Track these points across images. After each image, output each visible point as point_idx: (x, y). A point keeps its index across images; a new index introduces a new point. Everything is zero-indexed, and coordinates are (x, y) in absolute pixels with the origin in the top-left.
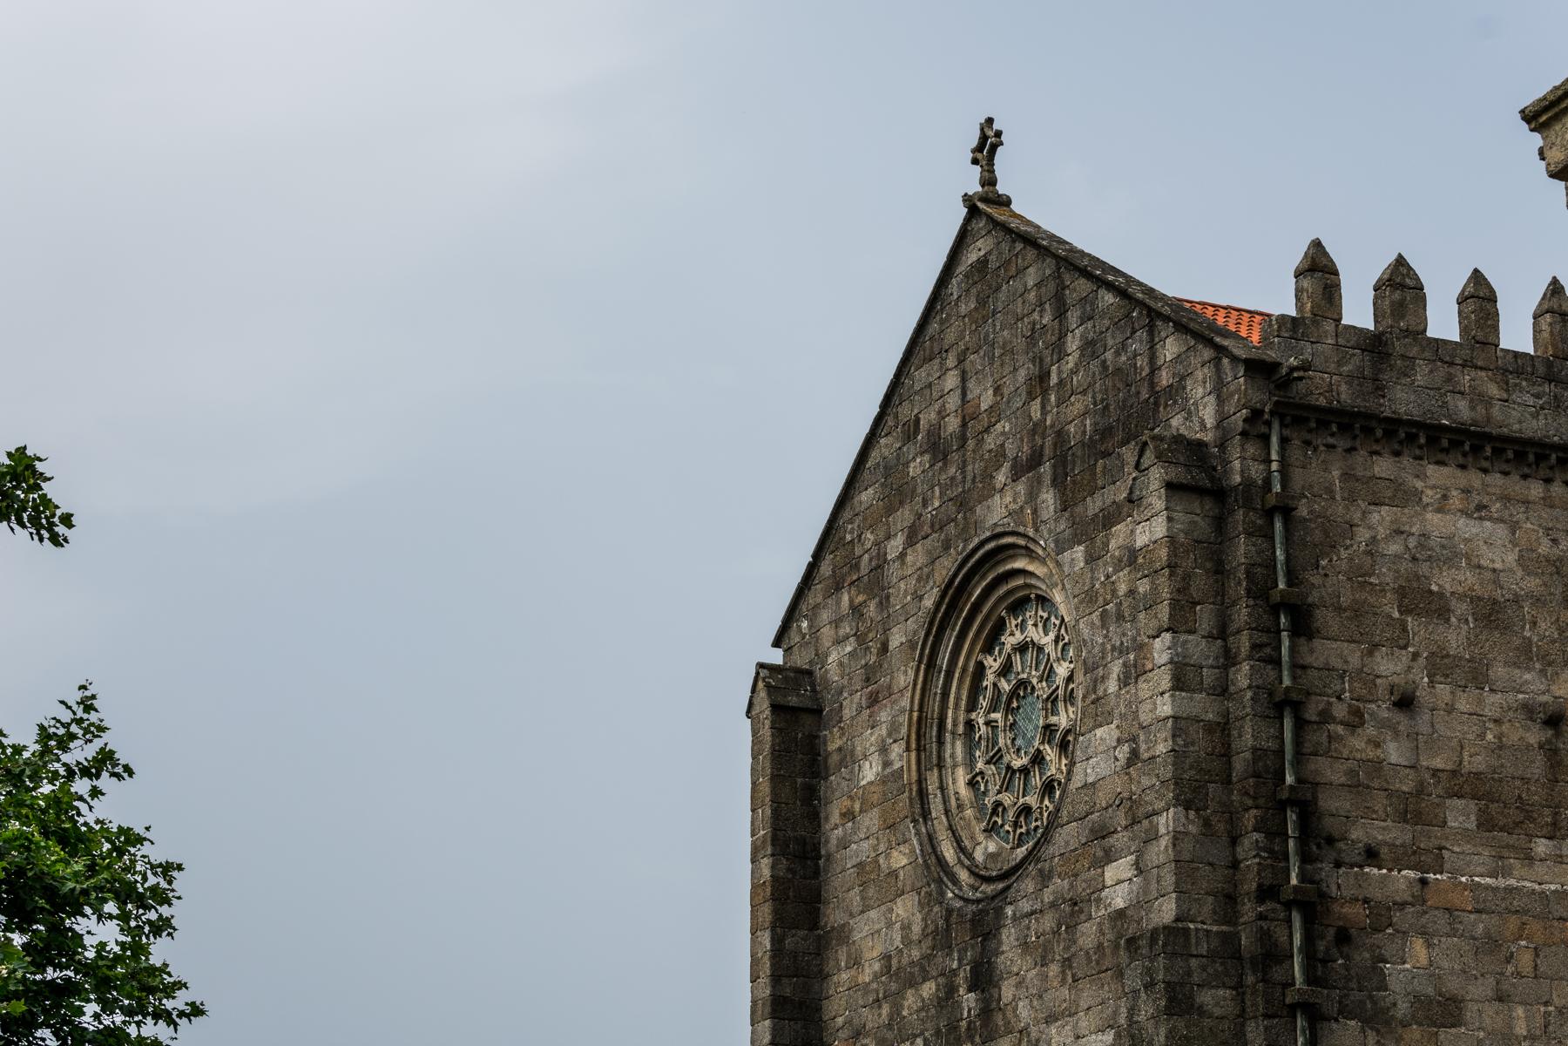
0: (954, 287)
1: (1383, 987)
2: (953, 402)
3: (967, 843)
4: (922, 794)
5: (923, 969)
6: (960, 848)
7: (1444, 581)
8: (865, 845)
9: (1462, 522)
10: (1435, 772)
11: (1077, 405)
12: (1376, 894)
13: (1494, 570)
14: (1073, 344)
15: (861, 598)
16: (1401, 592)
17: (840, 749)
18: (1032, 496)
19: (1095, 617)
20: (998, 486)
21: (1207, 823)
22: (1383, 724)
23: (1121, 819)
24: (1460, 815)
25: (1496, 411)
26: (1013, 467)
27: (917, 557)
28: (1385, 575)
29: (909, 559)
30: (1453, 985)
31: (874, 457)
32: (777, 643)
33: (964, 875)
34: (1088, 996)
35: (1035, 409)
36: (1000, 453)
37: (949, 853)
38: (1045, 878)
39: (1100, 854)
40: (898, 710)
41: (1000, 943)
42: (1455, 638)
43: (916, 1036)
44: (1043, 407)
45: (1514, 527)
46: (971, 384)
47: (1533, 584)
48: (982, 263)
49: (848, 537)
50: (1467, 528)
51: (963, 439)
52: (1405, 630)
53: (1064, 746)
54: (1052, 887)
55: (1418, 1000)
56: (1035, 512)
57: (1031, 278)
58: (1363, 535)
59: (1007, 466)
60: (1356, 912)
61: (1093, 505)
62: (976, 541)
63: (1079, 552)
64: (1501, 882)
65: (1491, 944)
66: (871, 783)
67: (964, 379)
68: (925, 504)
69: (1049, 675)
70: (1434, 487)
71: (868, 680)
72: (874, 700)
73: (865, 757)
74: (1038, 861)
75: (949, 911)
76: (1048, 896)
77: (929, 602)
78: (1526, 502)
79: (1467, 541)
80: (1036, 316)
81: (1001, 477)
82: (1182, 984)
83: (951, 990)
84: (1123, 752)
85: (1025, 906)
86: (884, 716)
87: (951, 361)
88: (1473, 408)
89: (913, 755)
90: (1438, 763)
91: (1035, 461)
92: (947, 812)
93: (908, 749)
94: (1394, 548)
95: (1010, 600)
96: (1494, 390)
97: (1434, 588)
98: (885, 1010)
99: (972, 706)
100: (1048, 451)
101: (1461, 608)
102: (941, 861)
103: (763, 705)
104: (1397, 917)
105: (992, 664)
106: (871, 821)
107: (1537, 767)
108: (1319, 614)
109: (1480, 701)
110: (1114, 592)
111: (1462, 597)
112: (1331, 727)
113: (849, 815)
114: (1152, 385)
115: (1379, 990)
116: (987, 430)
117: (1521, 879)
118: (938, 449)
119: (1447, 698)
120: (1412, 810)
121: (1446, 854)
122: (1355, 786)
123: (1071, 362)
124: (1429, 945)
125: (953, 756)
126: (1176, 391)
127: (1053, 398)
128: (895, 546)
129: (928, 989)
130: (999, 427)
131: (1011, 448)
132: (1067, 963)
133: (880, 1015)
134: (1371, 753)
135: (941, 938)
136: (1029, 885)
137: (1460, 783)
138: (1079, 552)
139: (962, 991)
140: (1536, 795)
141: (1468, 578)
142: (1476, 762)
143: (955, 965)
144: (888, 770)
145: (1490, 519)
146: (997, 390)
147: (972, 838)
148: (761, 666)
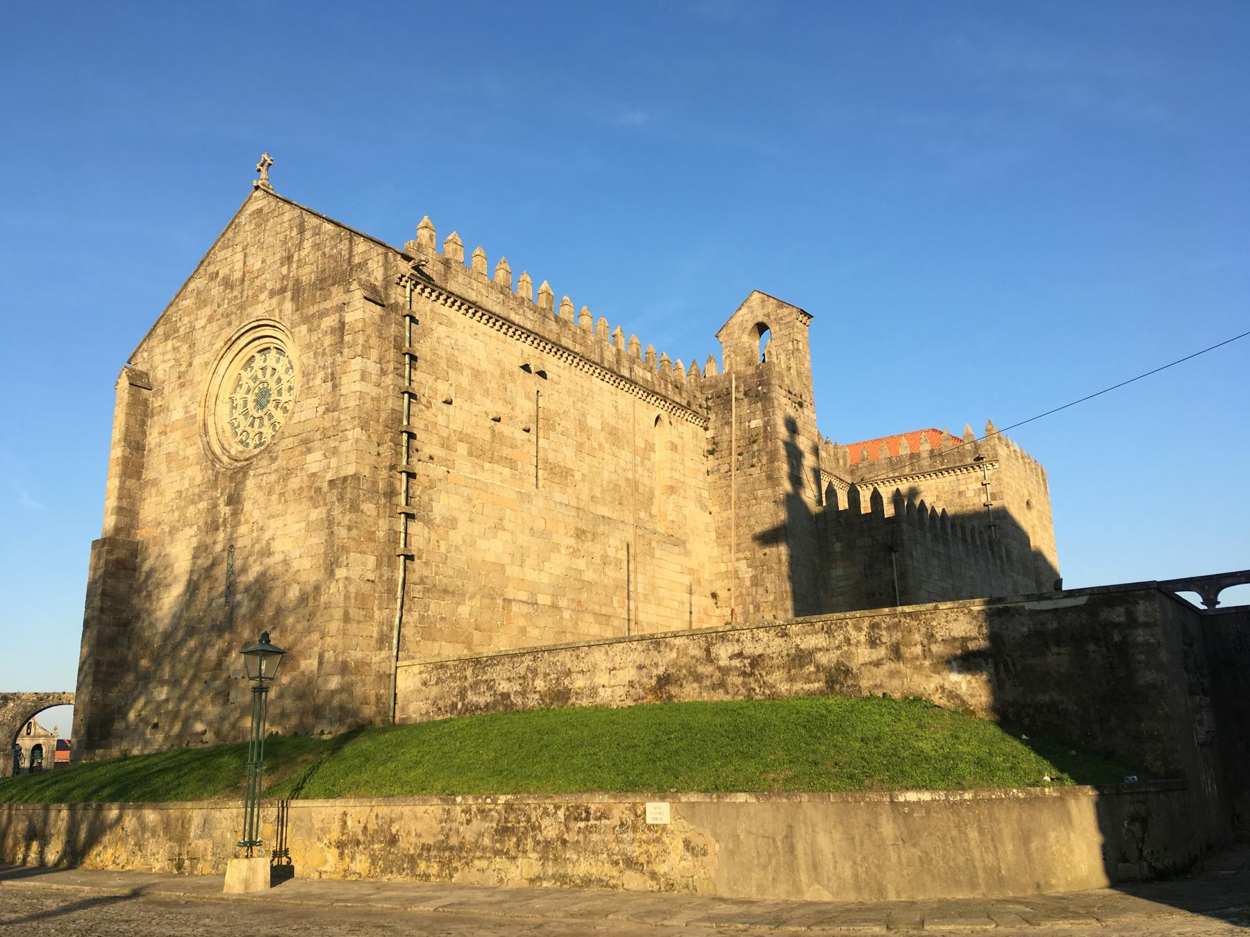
2: (239, 265)
3: (227, 446)
5: (200, 496)
7: (462, 359)
11: (308, 269)
14: (307, 245)
15: (179, 344)
17: (161, 406)
18: (280, 304)
19: (311, 355)
21: (369, 436)
22: (439, 409)
23: (318, 435)
24: (462, 448)
27: (214, 327)
29: (207, 329)
30: (456, 513)
33: (225, 459)
34: (293, 507)
35: (284, 270)
36: (262, 288)
37: (218, 450)
39: (305, 450)
41: (245, 486)
43: (192, 525)
44: (289, 269)
45: (486, 345)
46: (248, 259)
48: (260, 211)
49: (174, 319)
50: (471, 341)
51: (243, 280)
53: (285, 410)
54: (276, 463)
56: (280, 311)
57: (286, 217)
58: (436, 334)
59: (266, 293)
61: (313, 310)
62: (247, 322)
63: (304, 328)
64: (474, 476)
67: (245, 256)
68: (219, 306)
71: (179, 377)
72: (182, 385)
73: (175, 409)
74: (270, 452)
75: (218, 473)
78: (491, 337)
80: (288, 233)
83: (215, 506)
87: (239, 248)
88: (477, 296)
91: (283, 290)
94: (447, 342)
96: (484, 292)
98: (177, 514)
100: (290, 287)
102: (213, 453)
104: (438, 484)
107: (488, 437)
110: (322, 345)
114: (349, 262)
116: (257, 278)
120: (446, 444)
126: (362, 265)
127: (295, 266)
130: (263, 276)
131: (269, 285)
133: (173, 516)
134: (434, 419)
135: (214, 484)
136: (265, 462)
137: (463, 437)
139: (221, 506)
142: (469, 430)
143: (219, 495)
144: (188, 415)
146: (263, 261)
147: (230, 445)
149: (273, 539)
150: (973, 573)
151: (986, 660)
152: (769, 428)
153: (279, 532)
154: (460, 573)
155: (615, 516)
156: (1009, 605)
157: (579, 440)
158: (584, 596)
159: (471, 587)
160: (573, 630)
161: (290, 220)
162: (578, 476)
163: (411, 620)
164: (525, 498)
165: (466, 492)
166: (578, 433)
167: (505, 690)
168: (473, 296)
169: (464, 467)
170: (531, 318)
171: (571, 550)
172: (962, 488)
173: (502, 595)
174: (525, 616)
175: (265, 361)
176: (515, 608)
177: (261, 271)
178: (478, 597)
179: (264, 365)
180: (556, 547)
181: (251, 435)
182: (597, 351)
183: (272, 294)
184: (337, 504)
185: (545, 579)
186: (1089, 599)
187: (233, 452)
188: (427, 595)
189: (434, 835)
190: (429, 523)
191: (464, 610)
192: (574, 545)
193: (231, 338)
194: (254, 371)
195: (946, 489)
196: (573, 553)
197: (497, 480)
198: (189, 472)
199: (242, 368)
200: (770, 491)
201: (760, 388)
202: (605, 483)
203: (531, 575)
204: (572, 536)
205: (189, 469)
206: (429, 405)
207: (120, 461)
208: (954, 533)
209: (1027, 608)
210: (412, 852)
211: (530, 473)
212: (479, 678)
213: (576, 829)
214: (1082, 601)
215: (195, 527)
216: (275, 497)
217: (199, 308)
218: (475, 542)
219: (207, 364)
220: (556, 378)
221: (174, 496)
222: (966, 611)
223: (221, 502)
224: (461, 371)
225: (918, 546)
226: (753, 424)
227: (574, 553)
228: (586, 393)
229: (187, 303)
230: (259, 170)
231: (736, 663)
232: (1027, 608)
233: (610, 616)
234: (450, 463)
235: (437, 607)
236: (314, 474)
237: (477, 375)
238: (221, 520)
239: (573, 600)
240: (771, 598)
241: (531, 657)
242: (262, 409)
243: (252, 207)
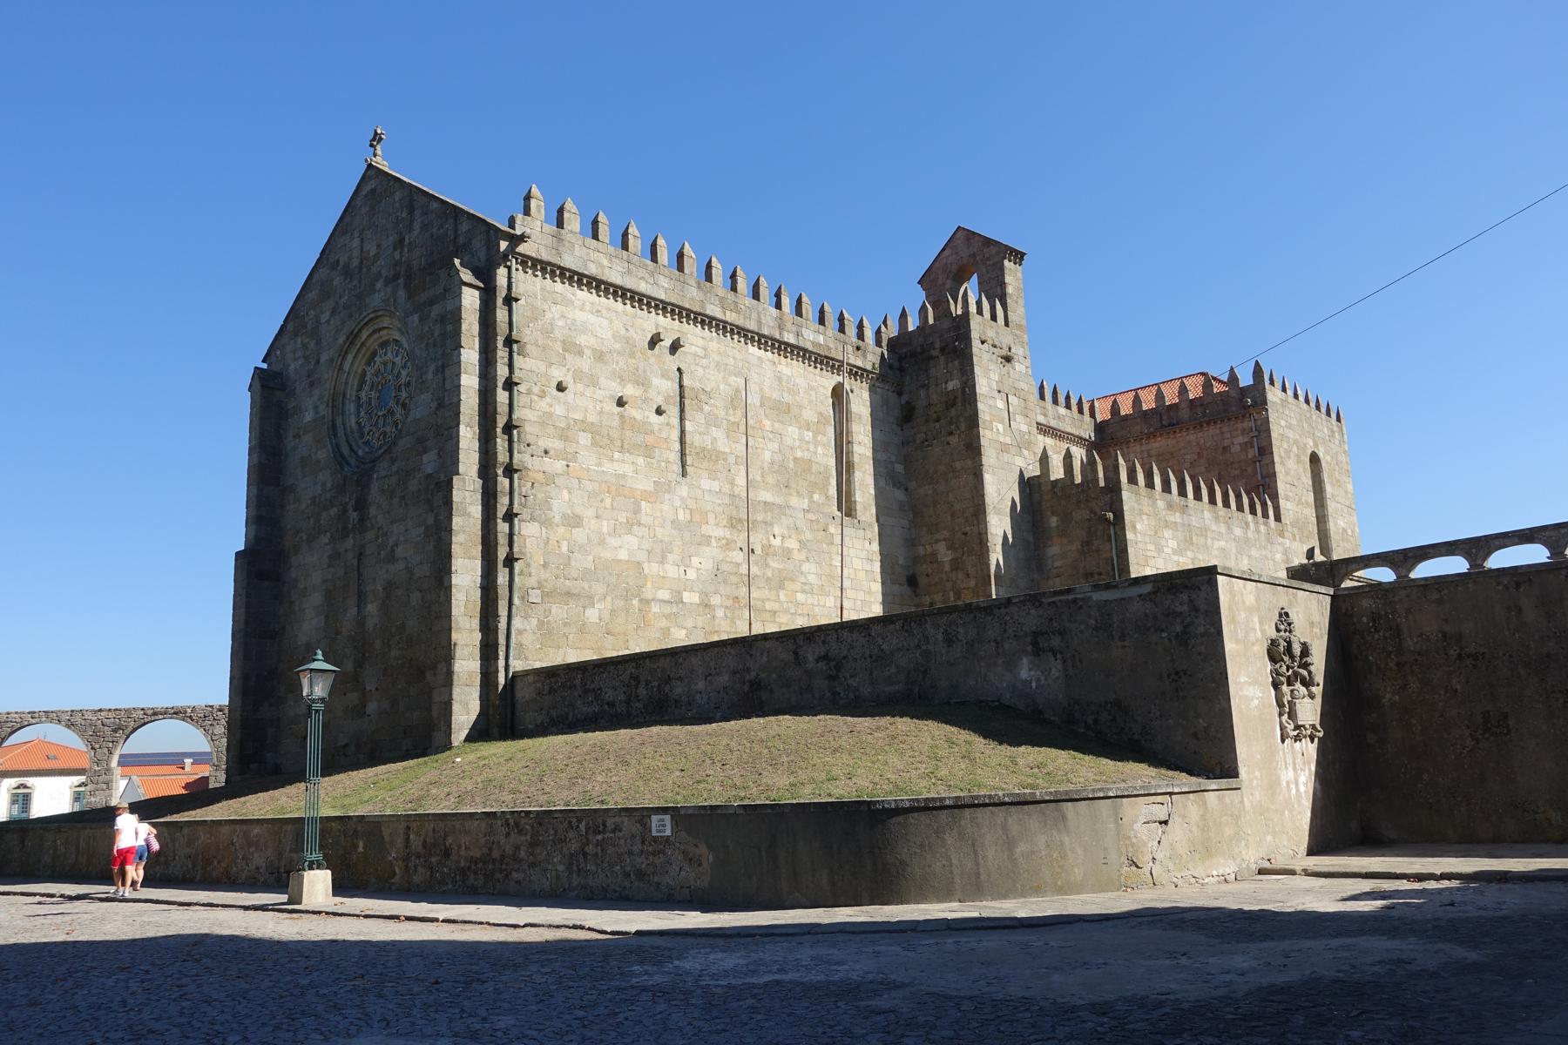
0: (359, 202)
1: (550, 509)
2: (356, 253)
3: (355, 448)
4: (334, 425)
6: (352, 449)
7: (582, 340)
9: (590, 316)
10: (575, 420)
12: (548, 469)
13: (602, 339)
14: (417, 226)
15: (307, 340)
16: (564, 342)
17: (294, 407)
20: (378, 289)
22: (554, 398)
24: (584, 439)
25: (607, 271)
26: (385, 280)
28: (558, 334)
29: (331, 322)
30: (578, 510)
31: (316, 277)
32: (264, 361)
33: (353, 461)
35: (397, 256)
37: (346, 451)
38: (393, 460)
39: (421, 449)
42: (585, 364)
43: (326, 532)
44: (401, 253)
45: (611, 322)
46: (365, 245)
47: (617, 346)
48: (373, 191)
49: (302, 313)
50: (592, 319)
51: (360, 268)
52: (565, 359)
53: (404, 406)
54: (396, 465)
55: (564, 516)
56: (395, 301)
58: (549, 315)
59: (382, 281)
60: (540, 476)
61: (423, 297)
62: (365, 314)
63: (416, 317)
65: (592, 495)
66: (309, 422)
67: (362, 241)
68: (340, 297)
70: (579, 300)
71: (309, 376)
72: (312, 384)
74: (390, 453)
76: (395, 468)
77: (341, 341)
79: (592, 324)
80: (399, 214)
81: (379, 285)
82: (462, 503)
83: (345, 511)
84: (433, 405)
85: (383, 473)
86: (317, 392)
87: (356, 234)
88: (597, 269)
89: (330, 409)
90: (576, 417)
91: (396, 277)
92: (345, 434)
93: (328, 406)
94: (561, 323)
95: (381, 341)
96: (605, 262)
97: (578, 343)
98: (312, 520)
99: (360, 389)
100: (402, 272)
101: (588, 352)
102: (342, 456)
103: (258, 386)
105: (370, 371)
106: (308, 438)
107: (616, 422)
108: (528, 347)
109: (594, 393)
110: (432, 334)
111: (588, 348)
112: (532, 396)
113: (297, 436)
115: (548, 510)
117: (608, 467)
118: (347, 273)
119: (581, 390)
120: (564, 437)
121: (578, 455)
122: (542, 424)
123: (416, 233)
124: (570, 493)
125: (349, 410)
127: (406, 250)
128: (325, 317)
129: (333, 511)
130: (378, 263)
131: (384, 273)
132: (402, 498)
136: (385, 464)
137: (586, 426)
138: (416, 317)
139: (350, 512)
140: (615, 434)
141: (592, 341)
142: (592, 418)
143: (347, 500)
144: (318, 416)
145: (602, 317)
146: (379, 246)
147: (358, 445)
148: (256, 368)
150: (1222, 543)
151: (1055, 656)
152: (967, 389)
153: (402, 539)
154: (586, 575)
155: (778, 501)
156: (1078, 596)
157: (732, 419)
159: (599, 589)
160: (729, 629)
162: (731, 460)
163: (528, 627)
164: (662, 488)
165: (589, 486)
166: (731, 412)
167: (611, 699)
168: (592, 270)
169: (587, 458)
170: (666, 285)
171: (724, 542)
172: (1226, 443)
173: (638, 595)
174: (667, 617)
176: (655, 608)
178: (609, 599)
180: (706, 540)
182: (754, 315)
183: (387, 282)
184: (443, 507)
186: (1154, 587)
188: (546, 599)
189: (480, 849)
190: (546, 523)
191: (592, 615)
192: (728, 536)
193: (353, 331)
194: (376, 366)
195: (1208, 445)
196: (727, 544)
197: (627, 469)
198: (321, 476)
199: (365, 364)
200: (969, 462)
201: (957, 344)
202: (766, 465)
203: (672, 571)
204: (725, 526)
206: (543, 395)
208: (1198, 497)
209: (1094, 599)
210: (462, 864)
211: (671, 460)
212: (588, 687)
213: (595, 842)
214: (1147, 588)
215: (328, 534)
216: (396, 500)
218: (604, 539)
219: (332, 360)
220: (700, 352)
221: (309, 502)
222: (1037, 604)
223: (350, 508)
224: (580, 353)
225: (1144, 517)
226: (951, 386)
227: (728, 545)
228: (740, 365)
231: (821, 665)
232: (1094, 599)
233: (775, 612)
234: (570, 456)
235: (558, 612)
237: (600, 356)
238: (350, 526)
239: (728, 597)
240: (972, 583)
241: (634, 664)
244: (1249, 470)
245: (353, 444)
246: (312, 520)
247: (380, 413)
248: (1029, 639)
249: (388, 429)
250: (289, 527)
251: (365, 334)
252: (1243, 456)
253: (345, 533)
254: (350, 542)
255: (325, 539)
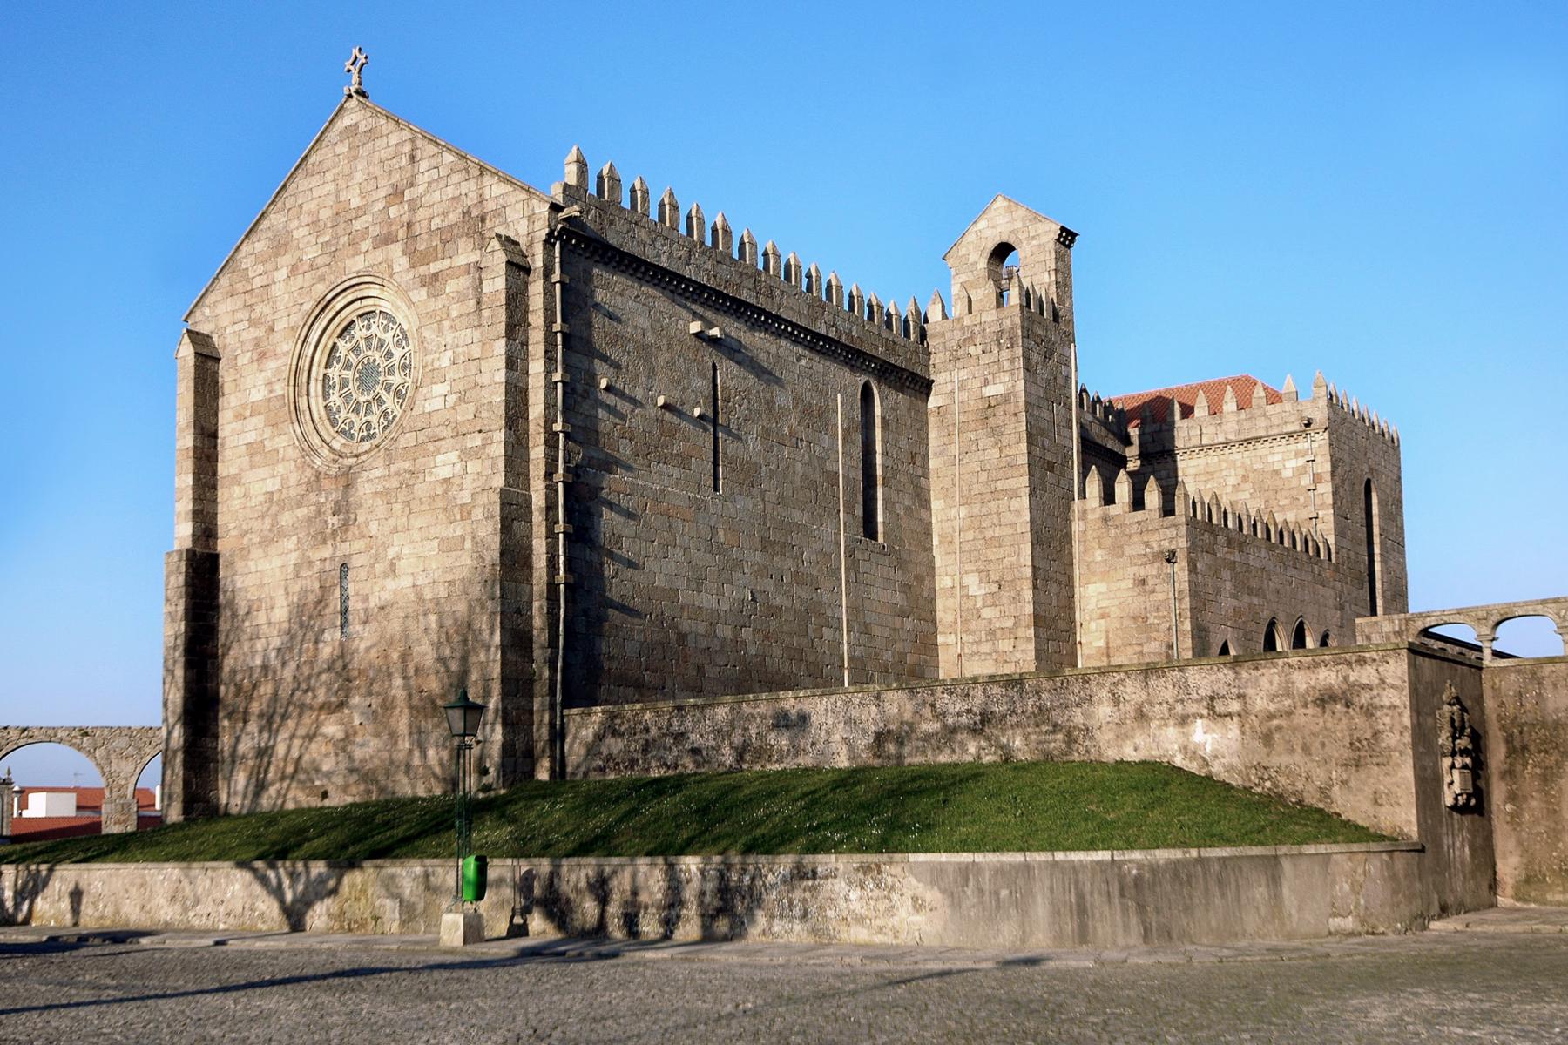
8: (253, 433)
15: (254, 300)
20: (363, 250)
27: (299, 281)
37: (316, 441)
38: (390, 458)
40: (279, 365)
53: (398, 393)
57: (394, 139)
61: (434, 267)
62: (345, 278)
69: (389, 355)
77: (308, 307)
98: (268, 521)
105: (344, 346)
116: (355, 218)
131: (375, 231)
132: (407, 503)
138: (424, 291)
149: (399, 558)
153: (406, 551)
158: (773, 623)
161: (397, 145)
175: (368, 329)
177: (361, 211)
179: (369, 333)
181: (356, 426)
185: (724, 605)
187: (336, 445)
195: (1255, 467)
205: (280, 466)
207: (191, 453)
217: (277, 255)
229: (259, 245)
230: (349, 71)
236: (447, 481)
242: (369, 391)
243: (346, 121)
244: (1302, 499)
245: (323, 433)
246: (268, 521)
247: (362, 399)
248: (1205, 703)
249: (373, 419)
250: (231, 526)
251: (339, 304)
252: (1294, 483)
253: (321, 538)
254: (326, 552)
255: (291, 543)
